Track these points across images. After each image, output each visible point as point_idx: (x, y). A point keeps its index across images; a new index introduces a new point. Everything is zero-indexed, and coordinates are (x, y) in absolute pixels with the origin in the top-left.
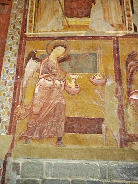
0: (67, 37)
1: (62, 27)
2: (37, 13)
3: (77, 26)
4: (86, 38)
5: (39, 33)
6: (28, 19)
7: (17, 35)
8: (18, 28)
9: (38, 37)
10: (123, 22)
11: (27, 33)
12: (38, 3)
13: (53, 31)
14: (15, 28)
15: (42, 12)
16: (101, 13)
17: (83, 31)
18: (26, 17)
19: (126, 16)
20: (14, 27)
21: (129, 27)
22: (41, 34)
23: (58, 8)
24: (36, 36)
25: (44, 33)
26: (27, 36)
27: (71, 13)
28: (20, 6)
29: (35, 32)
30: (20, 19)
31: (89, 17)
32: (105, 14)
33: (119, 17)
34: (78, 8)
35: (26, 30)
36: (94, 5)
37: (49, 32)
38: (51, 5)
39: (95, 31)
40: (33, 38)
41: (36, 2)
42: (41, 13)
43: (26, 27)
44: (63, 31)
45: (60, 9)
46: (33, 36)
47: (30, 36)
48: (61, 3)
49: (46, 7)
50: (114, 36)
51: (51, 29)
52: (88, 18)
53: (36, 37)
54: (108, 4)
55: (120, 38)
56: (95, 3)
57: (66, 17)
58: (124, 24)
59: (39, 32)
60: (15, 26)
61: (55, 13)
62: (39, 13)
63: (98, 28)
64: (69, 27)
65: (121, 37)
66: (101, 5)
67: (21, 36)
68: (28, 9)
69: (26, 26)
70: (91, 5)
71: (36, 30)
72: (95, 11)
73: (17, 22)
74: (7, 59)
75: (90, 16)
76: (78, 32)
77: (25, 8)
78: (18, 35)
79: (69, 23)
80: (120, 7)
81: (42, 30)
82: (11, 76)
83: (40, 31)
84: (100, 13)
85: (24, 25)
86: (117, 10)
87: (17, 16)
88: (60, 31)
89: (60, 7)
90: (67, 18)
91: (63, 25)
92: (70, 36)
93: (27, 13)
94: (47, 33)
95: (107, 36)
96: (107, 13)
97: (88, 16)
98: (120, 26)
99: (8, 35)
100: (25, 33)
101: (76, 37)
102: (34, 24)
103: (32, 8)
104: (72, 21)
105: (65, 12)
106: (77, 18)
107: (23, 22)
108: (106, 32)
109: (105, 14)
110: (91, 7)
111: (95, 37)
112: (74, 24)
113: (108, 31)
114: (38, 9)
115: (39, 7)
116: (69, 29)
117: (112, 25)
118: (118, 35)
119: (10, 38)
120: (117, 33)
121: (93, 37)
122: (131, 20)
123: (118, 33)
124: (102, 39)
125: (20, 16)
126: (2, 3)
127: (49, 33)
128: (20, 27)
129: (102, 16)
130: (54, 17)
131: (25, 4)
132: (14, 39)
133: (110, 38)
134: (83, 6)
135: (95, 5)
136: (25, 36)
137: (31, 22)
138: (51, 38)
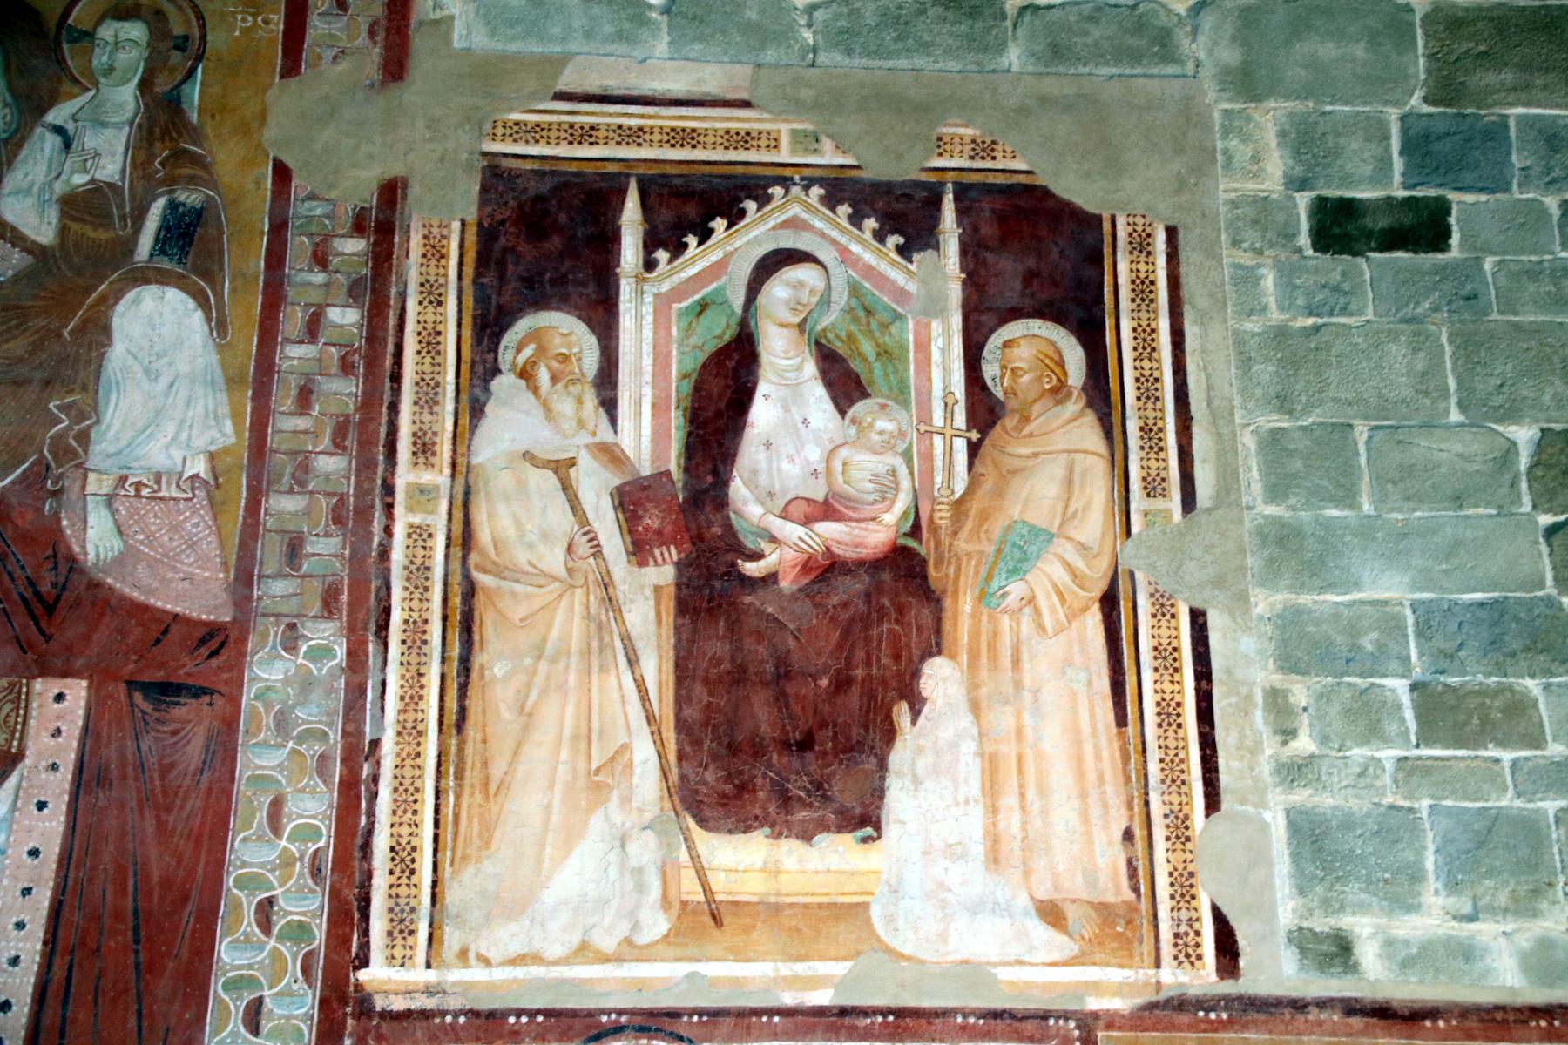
0: (700, 1012)
1: (656, 925)
2: (459, 776)
3: (777, 908)
4: (847, 1020)
5: (477, 974)
6: (381, 842)
7: (291, 994)
8: (301, 924)
9: (474, 1014)
10: (1136, 890)
11: (375, 974)
12: (463, 689)
13: (584, 951)
14: (279, 924)
15: (497, 770)
16: (967, 802)
17: (822, 958)
18: (363, 821)
19: (1159, 833)
20: (265, 911)
21: (1177, 935)
22: (491, 986)
23: (622, 739)
24: (454, 1003)
25: (519, 972)
26: (379, 1003)
27: (728, 788)
28: (308, 715)
29: (443, 965)
30: (317, 833)
31: (869, 831)
32: (993, 810)
33: (1100, 838)
34: (785, 745)
35: (365, 946)
36: (916, 714)
37: (556, 963)
38: (570, 711)
39: (922, 962)
40: (425, 1015)
41: (443, 677)
42: (486, 784)
43: (366, 917)
44: (672, 952)
45: (644, 752)
46: (430, 1003)
47: (398, 1004)
48: (653, 694)
49: (526, 729)
50: (1066, 1016)
51: (576, 940)
52: (865, 840)
53: (456, 1015)
54: (1019, 715)
55: (1109, 1026)
56: (923, 701)
57: (691, 823)
58: (1144, 905)
59: (472, 955)
60: (270, 901)
61: (601, 779)
62: (472, 776)
63: (943, 937)
64: (716, 918)
65: (1112, 1021)
66: (966, 721)
67: (324, 1003)
68: (376, 744)
69: (365, 901)
70: (888, 716)
71: (452, 938)
72: (917, 781)
73: (287, 862)
75: (877, 827)
76: (785, 969)
77: (352, 736)
78: (300, 986)
79: (718, 882)
80: (1110, 741)
81: (505, 938)
83: (483, 952)
84: (961, 799)
85: (351, 894)
86: (1091, 776)
87: (290, 807)
88: (644, 954)
89: (645, 730)
90: (697, 833)
91: (666, 902)
92: (721, 1004)
93: (375, 779)
94: (536, 971)
95: (1010, 1014)
96: (1009, 800)
97: (864, 819)
98: (1113, 925)
99: (217, 987)
100: (363, 975)
101: (771, 1012)
102: (435, 884)
103: (411, 731)
104: (744, 860)
105: (683, 777)
106: (778, 836)
107: (341, 862)
108: (1004, 974)
109: (993, 810)
110: (890, 734)
111: (916, 1013)
112: (752, 888)
113: (1020, 963)
114: (461, 750)
115: (471, 731)
116: (716, 932)
117: (1052, 914)
118: (1093, 1004)
119: (236, 1022)
120: (1087, 984)
121: (900, 1013)
122: (1191, 868)
123: (1096, 988)
124: (967, 1032)
125: (313, 808)
126: (159, 675)
127: (557, 972)
128: (305, 906)
129: (973, 823)
130: (596, 823)
131: (356, 694)
132: (266, 1026)
133: (1029, 1027)
134: (823, 725)
135: (921, 720)
136: (364, 1005)
137: (403, 860)
138: (578, 1024)
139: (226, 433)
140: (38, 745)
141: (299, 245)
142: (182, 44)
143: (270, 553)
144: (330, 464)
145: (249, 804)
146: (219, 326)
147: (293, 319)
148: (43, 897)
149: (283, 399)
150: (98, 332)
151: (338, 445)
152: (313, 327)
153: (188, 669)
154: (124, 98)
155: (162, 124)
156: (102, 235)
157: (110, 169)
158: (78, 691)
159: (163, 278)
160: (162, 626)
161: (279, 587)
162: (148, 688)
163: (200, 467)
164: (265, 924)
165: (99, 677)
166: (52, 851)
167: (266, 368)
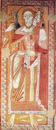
74: (50, 81)
82: (52, 88)
139: (46, 38)
140: (38, 56)
141: (50, 26)
142: (42, 13)
143: (49, 45)
144: (52, 40)
145: (49, 59)
146: (46, 32)
147: (50, 31)
148: (40, 64)
149: (49, 36)
150: (39, 32)
151: (53, 39)
152: (51, 31)
153: (45, 52)
154: (39, 16)
155: (41, 17)
156: (39, 25)
157: (39, 21)
158: (40, 53)
159: (42, 28)
160: (44, 50)
161: (50, 47)
162: (44, 53)
163: (45, 40)
164: (51, 66)
165: (41, 53)
166: (40, 62)
167: (48, 34)
